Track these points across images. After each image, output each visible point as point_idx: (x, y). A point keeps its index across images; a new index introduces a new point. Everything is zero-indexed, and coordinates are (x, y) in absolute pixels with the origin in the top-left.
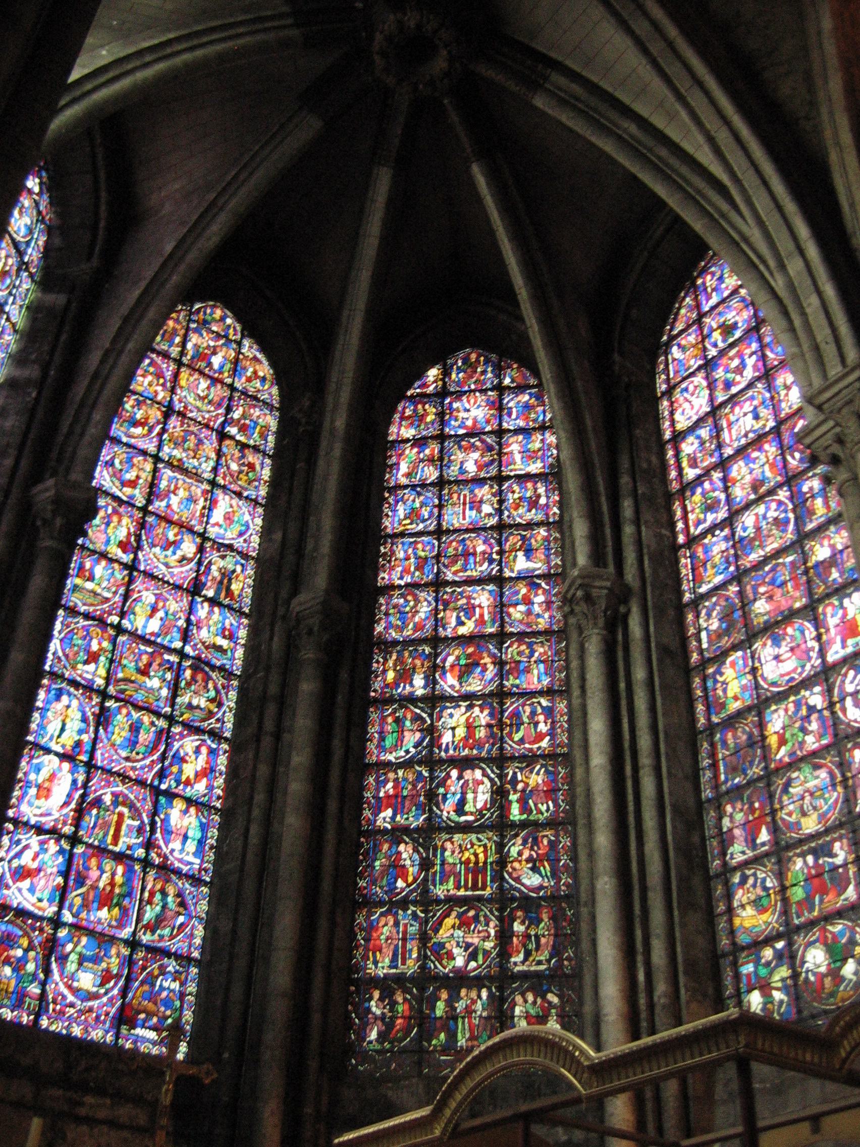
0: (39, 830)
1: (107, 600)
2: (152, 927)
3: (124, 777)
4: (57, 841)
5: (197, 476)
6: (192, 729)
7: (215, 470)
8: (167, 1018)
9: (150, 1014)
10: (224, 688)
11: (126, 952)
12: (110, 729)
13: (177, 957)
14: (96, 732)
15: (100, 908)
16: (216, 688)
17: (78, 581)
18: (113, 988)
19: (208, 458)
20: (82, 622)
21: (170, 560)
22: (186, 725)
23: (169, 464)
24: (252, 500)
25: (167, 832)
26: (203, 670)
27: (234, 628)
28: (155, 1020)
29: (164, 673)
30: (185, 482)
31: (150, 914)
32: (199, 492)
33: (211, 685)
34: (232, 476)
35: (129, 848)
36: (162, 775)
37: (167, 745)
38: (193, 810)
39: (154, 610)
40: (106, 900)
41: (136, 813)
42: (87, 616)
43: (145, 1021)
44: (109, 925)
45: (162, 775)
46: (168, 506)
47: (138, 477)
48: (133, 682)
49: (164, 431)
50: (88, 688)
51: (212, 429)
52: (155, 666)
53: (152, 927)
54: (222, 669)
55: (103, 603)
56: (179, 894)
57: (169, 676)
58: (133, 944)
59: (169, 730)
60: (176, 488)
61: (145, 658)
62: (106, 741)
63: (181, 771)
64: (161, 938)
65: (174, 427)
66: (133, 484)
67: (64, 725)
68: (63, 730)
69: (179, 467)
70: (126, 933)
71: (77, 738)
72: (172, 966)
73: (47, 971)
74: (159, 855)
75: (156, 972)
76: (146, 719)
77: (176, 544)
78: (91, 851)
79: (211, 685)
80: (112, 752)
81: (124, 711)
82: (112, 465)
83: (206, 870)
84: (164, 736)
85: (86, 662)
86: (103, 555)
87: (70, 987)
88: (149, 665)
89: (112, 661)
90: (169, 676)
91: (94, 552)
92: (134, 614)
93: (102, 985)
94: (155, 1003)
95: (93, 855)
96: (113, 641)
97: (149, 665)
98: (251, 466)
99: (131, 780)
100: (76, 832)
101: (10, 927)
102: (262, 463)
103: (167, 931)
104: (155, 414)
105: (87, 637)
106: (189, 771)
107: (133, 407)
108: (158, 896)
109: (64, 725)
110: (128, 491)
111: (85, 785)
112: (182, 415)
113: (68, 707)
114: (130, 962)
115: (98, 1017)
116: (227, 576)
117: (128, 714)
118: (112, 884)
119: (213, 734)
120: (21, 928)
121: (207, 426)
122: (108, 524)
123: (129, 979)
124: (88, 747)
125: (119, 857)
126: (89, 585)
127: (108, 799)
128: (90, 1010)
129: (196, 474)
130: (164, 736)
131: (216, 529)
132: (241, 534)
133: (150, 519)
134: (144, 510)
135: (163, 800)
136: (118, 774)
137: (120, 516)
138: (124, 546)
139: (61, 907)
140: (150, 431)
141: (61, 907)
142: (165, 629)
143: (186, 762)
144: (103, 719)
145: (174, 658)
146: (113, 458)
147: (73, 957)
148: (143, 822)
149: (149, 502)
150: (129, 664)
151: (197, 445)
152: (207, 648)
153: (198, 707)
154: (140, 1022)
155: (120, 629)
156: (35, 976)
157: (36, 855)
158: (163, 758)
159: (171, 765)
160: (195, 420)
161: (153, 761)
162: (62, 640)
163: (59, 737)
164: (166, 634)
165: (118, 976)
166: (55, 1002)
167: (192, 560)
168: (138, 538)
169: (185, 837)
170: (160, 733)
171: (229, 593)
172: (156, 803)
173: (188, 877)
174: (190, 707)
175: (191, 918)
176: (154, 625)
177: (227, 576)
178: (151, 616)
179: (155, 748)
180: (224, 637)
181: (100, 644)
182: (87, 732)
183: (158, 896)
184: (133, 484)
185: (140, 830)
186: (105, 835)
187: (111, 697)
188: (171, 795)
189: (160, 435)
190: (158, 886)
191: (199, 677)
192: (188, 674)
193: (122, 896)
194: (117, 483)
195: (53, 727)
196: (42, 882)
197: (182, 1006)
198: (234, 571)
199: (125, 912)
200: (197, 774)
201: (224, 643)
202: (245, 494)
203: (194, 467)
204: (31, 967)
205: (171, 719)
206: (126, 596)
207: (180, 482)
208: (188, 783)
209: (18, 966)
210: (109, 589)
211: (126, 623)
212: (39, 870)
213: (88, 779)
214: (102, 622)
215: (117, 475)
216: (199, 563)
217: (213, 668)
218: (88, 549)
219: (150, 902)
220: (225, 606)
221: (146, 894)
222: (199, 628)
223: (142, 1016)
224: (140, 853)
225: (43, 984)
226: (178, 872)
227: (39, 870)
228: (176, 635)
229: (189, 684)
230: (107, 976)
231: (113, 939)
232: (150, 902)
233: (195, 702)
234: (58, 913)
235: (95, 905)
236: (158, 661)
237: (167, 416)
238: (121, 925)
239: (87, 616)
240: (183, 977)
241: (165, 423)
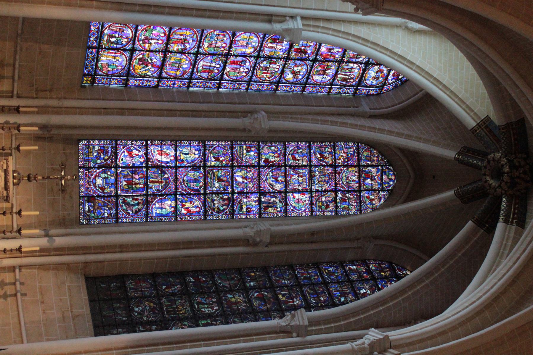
0: (146, 154)
1: (242, 159)
2: (124, 202)
3: (176, 180)
4: (144, 161)
5: (311, 185)
6: (204, 203)
7: (317, 191)
8: (94, 213)
9: (94, 207)
10: (226, 212)
11: (113, 194)
12: (192, 172)
13: (117, 213)
14: (189, 167)
15: (125, 181)
16: (224, 210)
17: (245, 147)
18: (99, 191)
19: (321, 187)
20: (229, 152)
21: (271, 181)
22: (205, 199)
23: (310, 172)
24: (312, 210)
25: (161, 201)
26: (229, 203)
27: (252, 212)
28: (92, 209)
29: (223, 187)
30: (306, 179)
31: (129, 200)
32: (305, 186)
33: (225, 207)
34: (319, 199)
35: (151, 188)
36: (182, 194)
37: (195, 194)
38: (173, 209)
39: (246, 178)
40: (129, 183)
41: (164, 188)
42: (232, 153)
43: (91, 205)
44: (121, 186)
45: (182, 194)
46: (292, 175)
47: (298, 160)
48: (214, 176)
49: (324, 166)
50: (205, 160)
51: (336, 186)
52: (224, 183)
53: (124, 202)
54: (234, 211)
55: (240, 158)
56: (140, 210)
57: (222, 189)
58: (117, 196)
59: (201, 194)
60: (302, 177)
61: (225, 179)
62: (187, 171)
63: (186, 202)
64: (122, 206)
65: (328, 170)
66: (294, 159)
67: (188, 154)
68: (186, 154)
69: (311, 176)
70: (120, 193)
71: (184, 160)
72: (113, 212)
73: (99, 168)
74: (151, 199)
75: (109, 206)
76: (201, 184)
77: (277, 181)
78: (145, 174)
79: (225, 207)
80: (184, 174)
81: (201, 175)
82: (298, 149)
83: (152, 219)
84: (197, 193)
85: (214, 157)
86: (259, 154)
87: (95, 176)
88: (223, 181)
89: (218, 166)
90: (222, 189)
91: (259, 150)
92: (241, 171)
93: (99, 187)
94: (98, 208)
95: (144, 175)
96: (226, 166)
97: (223, 181)
98: (327, 206)
99: (176, 183)
100: (150, 167)
101: (110, 152)
102: (332, 211)
103: (125, 208)
104: (330, 161)
105: (224, 155)
106: (188, 205)
107: (328, 151)
108: (136, 202)
109: (188, 154)
110: (290, 157)
111: (168, 167)
112: (336, 172)
113: (194, 154)
114: (110, 196)
115: (88, 188)
116: (273, 205)
117: (201, 177)
118: (136, 184)
119: (205, 212)
120: (111, 155)
121: (336, 184)
122: (272, 152)
123: (104, 197)
124: (182, 165)
125: (146, 184)
126: (245, 151)
127: (166, 176)
128: (90, 185)
129: (312, 184)
130: (197, 193)
131: (292, 197)
132: (294, 207)
133: (283, 169)
134: (285, 166)
135: (173, 197)
136: (176, 178)
137: (279, 156)
138: (266, 161)
139: (122, 167)
140: (321, 160)
141: (122, 167)
142: (239, 184)
143: (191, 203)
144: (195, 168)
145: (230, 191)
146: (301, 148)
147: (106, 175)
148: (162, 191)
149: (290, 167)
150: (221, 173)
151: (325, 181)
152: (239, 202)
153: (214, 204)
154: (90, 204)
155: (232, 167)
156: (97, 163)
157: (138, 155)
158: (190, 194)
159: (187, 198)
160: (336, 178)
161: (186, 190)
162: (218, 146)
163: (182, 153)
164: (238, 185)
165: (104, 193)
166: (89, 172)
167: (273, 189)
168: (273, 166)
169: (162, 208)
170: (198, 190)
171: (266, 208)
172: (170, 194)
173: (147, 212)
174: (213, 201)
175: (132, 216)
176: (240, 180)
177: (273, 205)
178: (242, 178)
179: (192, 190)
180: (247, 209)
181: (224, 160)
182: (188, 163)
183: (136, 202)
184: (294, 159)
185: (158, 190)
186: (153, 178)
187: (205, 169)
188: (176, 200)
189: (322, 165)
190: (140, 201)
191: (226, 202)
192: (226, 197)
193: (132, 189)
194: (292, 152)
195: (185, 150)
196: (128, 159)
197: (99, 219)
198: (277, 208)
199: (127, 191)
200: (187, 208)
201: (244, 209)
202: (313, 206)
203: (314, 182)
204: (99, 161)
205: (205, 194)
206: (247, 166)
207: (305, 178)
208: (183, 206)
209: (98, 157)
210: (246, 159)
211: (235, 169)
212: (132, 157)
213: (171, 167)
214: (232, 160)
215: (295, 151)
216: (274, 193)
217: (232, 206)
218: (259, 148)
219: (133, 199)
220: (260, 206)
221: (136, 197)
222: (246, 198)
223: (92, 204)
224: (150, 192)
225: (94, 167)
226: (147, 208)
227: (132, 157)
228: (239, 189)
229: (221, 198)
230: (103, 189)
231: (116, 188)
232: (133, 199)
233: (216, 202)
234: (119, 167)
235: (126, 179)
236: (226, 184)
237: (331, 166)
238: (122, 190)
239: (232, 153)
240: (110, 217)
241: (328, 166)
